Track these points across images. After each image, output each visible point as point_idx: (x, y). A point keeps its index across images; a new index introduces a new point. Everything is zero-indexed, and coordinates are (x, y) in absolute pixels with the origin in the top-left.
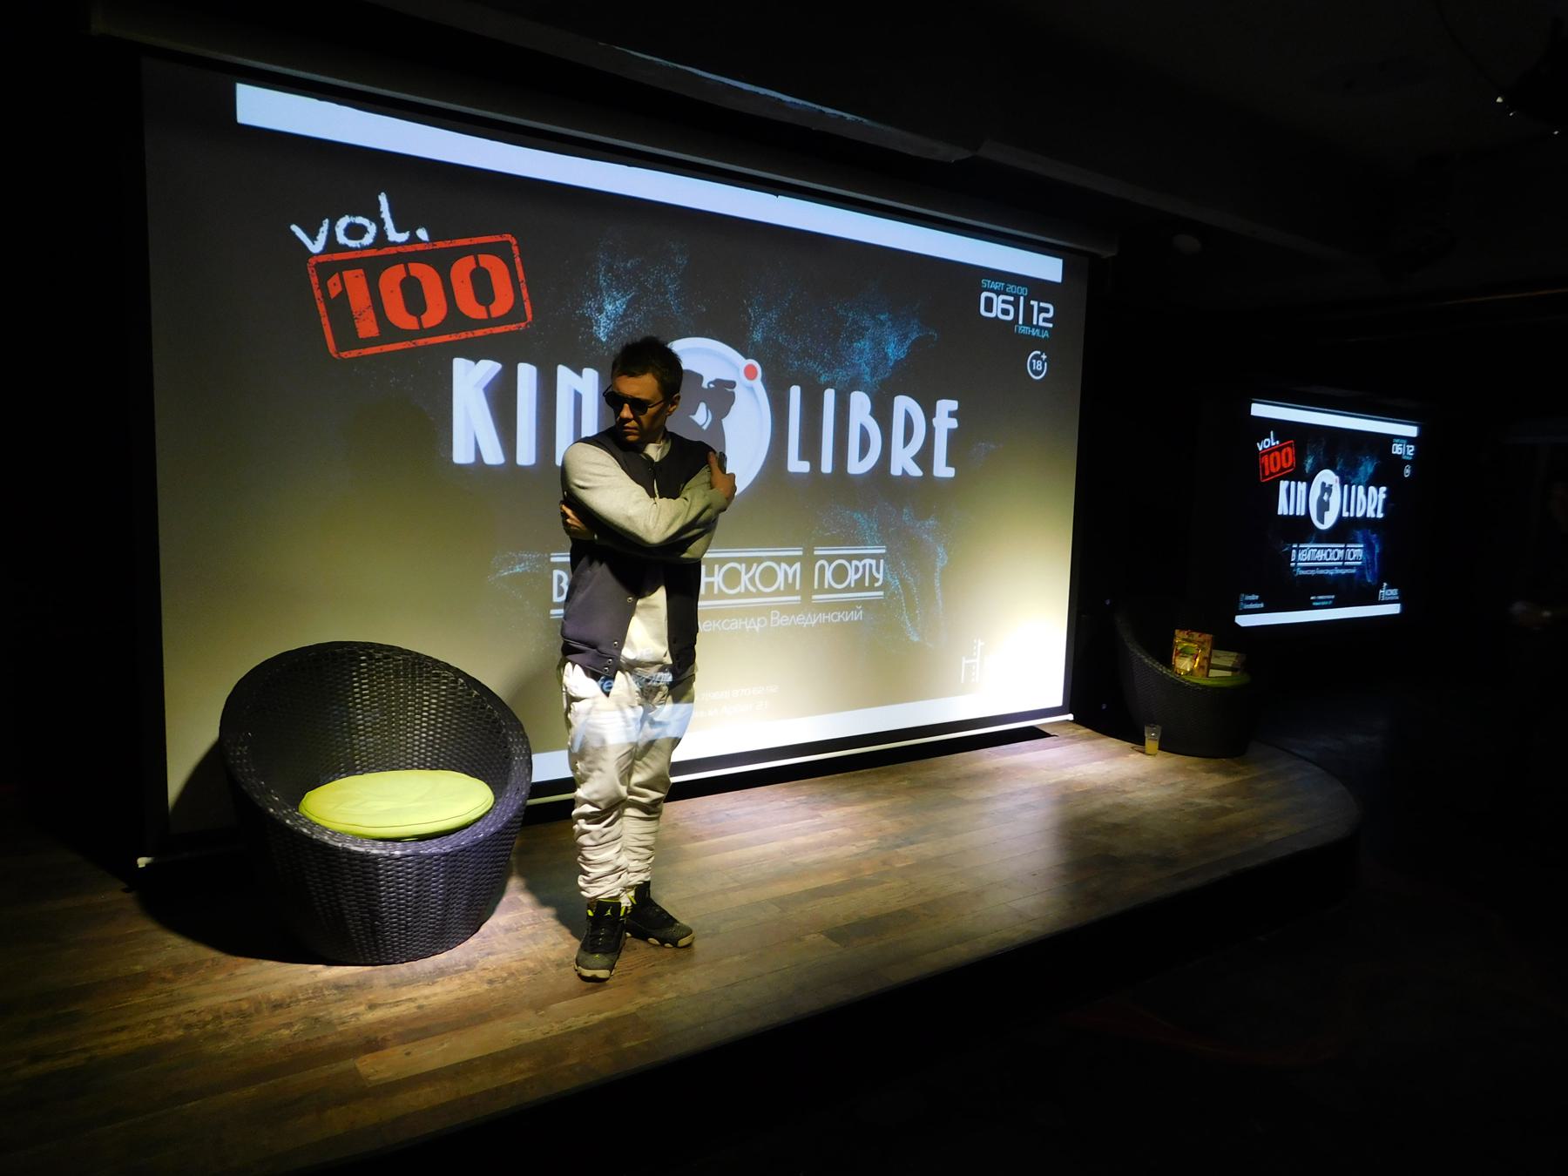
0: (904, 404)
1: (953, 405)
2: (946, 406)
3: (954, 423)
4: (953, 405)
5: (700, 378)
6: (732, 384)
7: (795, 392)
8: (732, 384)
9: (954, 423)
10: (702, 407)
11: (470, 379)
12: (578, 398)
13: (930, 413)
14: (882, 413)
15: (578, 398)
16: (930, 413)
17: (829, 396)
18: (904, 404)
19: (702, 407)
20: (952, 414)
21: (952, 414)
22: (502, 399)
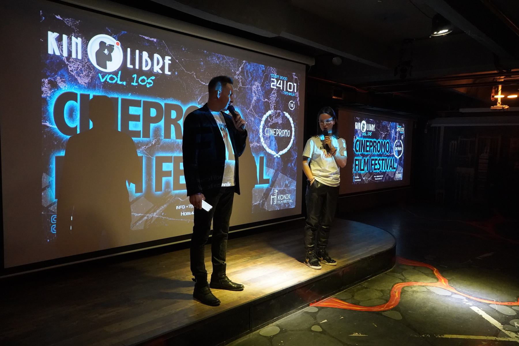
0: (156, 56)
1: (170, 58)
2: (167, 58)
3: (170, 62)
4: (170, 58)
5: (106, 43)
6: (113, 46)
7: (129, 50)
8: (113, 46)
9: (170, 62)
10: (106, 50)
11: (52, 36)
12: (77, 44)
13: (163, 59)
14: (151, 57)
15: (77, 44)
16: (163, 59)
17: (137, 51)
18: (156, 56)
19: (106, 50)
20: (169, 60)
21: (169, 60)
22: (59, 40)
